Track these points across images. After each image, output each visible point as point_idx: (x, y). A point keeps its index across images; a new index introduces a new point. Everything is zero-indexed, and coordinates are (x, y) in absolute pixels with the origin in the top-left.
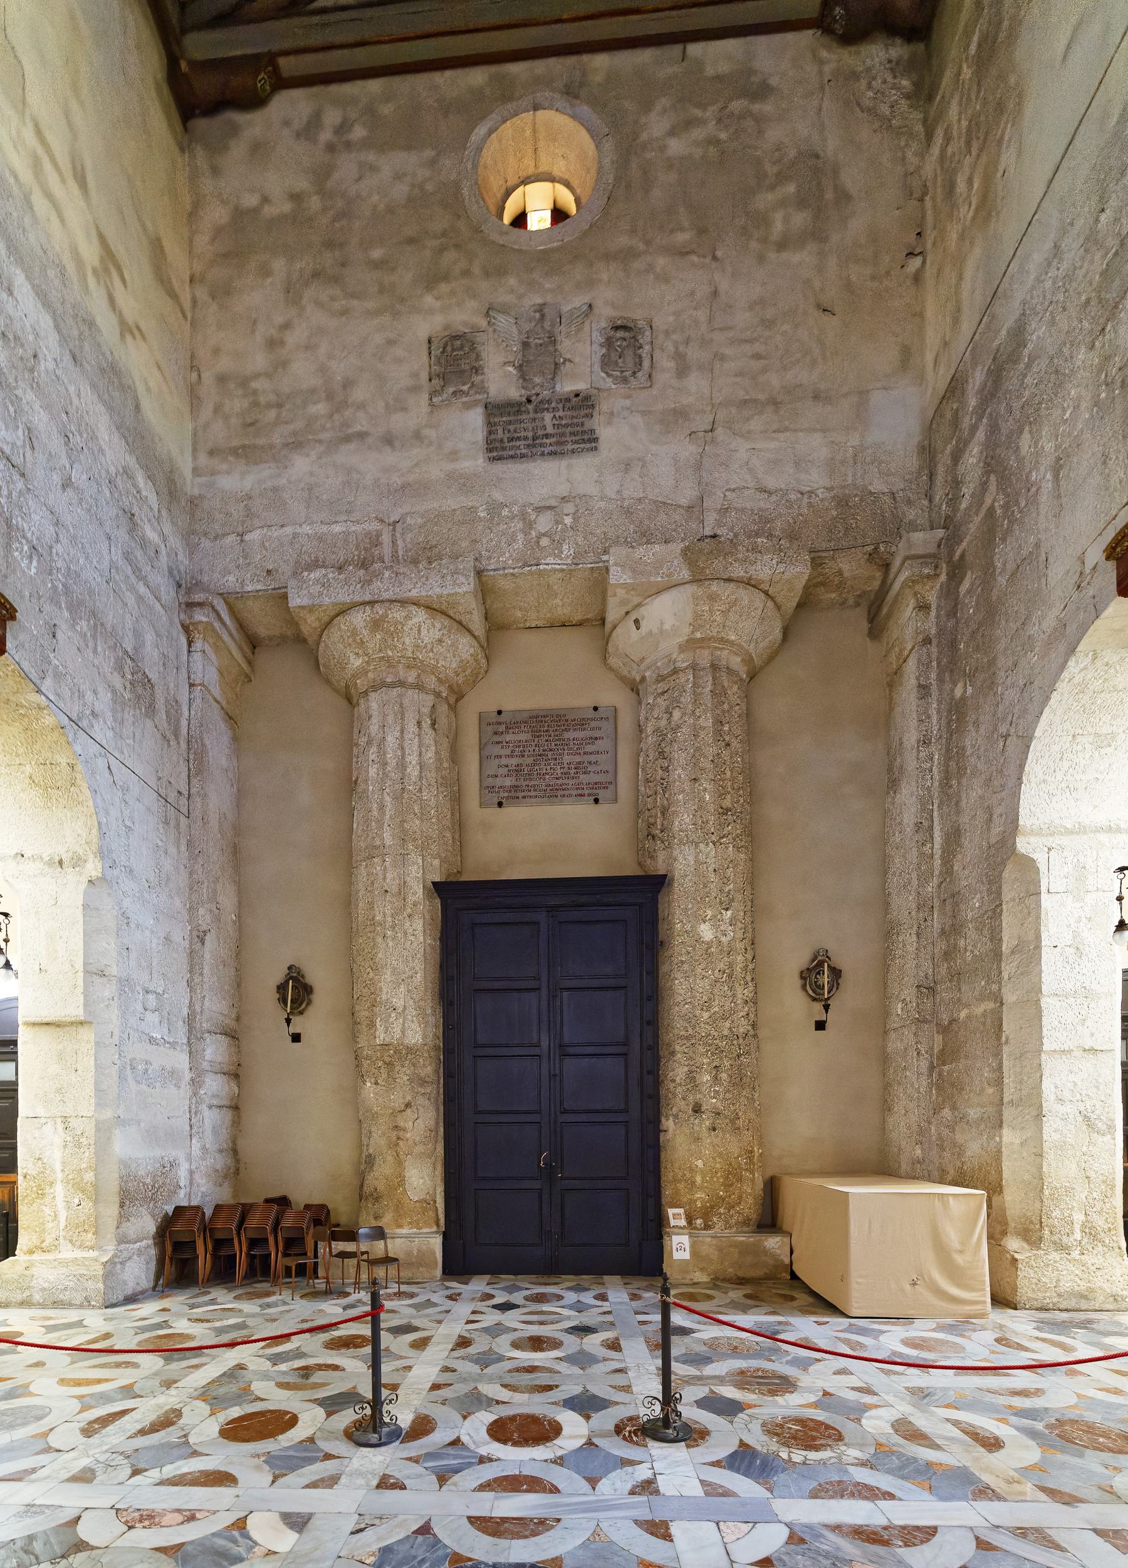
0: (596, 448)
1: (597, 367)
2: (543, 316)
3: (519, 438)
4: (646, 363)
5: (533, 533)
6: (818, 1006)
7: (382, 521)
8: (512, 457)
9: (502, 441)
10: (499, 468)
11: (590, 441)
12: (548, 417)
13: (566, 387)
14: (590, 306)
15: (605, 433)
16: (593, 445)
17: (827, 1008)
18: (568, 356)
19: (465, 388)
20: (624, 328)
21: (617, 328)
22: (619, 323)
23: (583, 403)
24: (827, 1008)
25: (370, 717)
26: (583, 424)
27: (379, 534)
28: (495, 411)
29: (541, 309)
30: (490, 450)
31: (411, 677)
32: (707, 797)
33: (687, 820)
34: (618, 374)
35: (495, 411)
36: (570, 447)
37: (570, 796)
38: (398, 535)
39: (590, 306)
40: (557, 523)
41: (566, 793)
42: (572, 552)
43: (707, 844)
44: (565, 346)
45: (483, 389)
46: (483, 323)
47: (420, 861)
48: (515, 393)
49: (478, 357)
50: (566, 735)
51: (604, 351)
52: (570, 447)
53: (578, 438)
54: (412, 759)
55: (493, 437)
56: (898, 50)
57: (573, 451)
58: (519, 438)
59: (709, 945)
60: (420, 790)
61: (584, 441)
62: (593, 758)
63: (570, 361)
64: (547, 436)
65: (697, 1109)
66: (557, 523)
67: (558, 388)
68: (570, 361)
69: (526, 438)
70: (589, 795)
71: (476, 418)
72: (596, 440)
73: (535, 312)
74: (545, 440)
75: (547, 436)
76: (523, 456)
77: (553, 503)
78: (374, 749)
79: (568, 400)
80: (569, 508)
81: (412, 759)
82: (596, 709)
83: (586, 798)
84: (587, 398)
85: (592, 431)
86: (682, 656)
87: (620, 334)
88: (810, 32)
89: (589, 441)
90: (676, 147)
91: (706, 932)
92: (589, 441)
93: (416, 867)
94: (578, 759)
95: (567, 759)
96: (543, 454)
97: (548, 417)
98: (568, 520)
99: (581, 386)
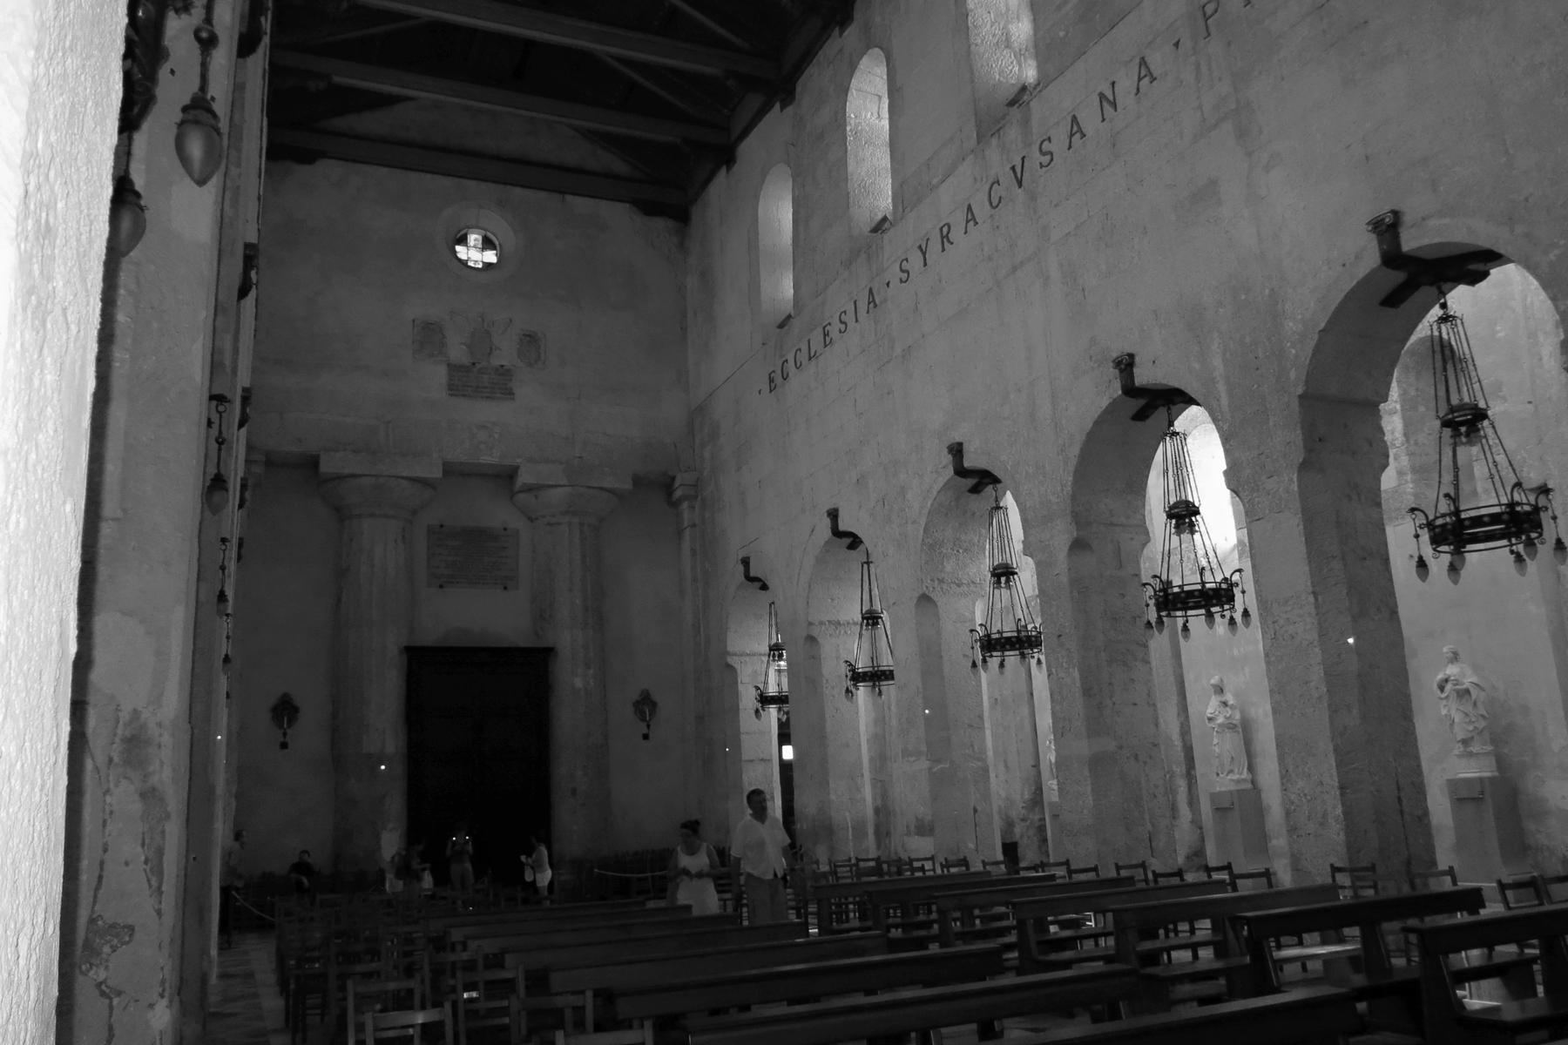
0: (513, 399)
2: (483, 320)
3: (468, 386)
6: (644, 725)
13: (496, 361)
14: (511, 320)
17: (648, 726)
20: (529, 336)
21: (525, 335)
22: (527, 333)
23: (505, 373)
24: (648, 726)
28: (453, 368)
30: (450, 389)
35: (453, 368)
39: (511, 320)
40: (490, 436)
48: (466, 361)
49: (444, 337)
58: (468, 386)
64: (486, 387)
65: (574, 792)
66: (490, 436)
69: (471, 386)
75: (486, 387)
79: (497, 369)
84: (509, 370)
85: (511, 389)
87: (528, 338)
88: (628, 205)
89: (509, 394)
92: (509, 394)
96: (482, 397)
97: (486, 377)
98: (497, 436)
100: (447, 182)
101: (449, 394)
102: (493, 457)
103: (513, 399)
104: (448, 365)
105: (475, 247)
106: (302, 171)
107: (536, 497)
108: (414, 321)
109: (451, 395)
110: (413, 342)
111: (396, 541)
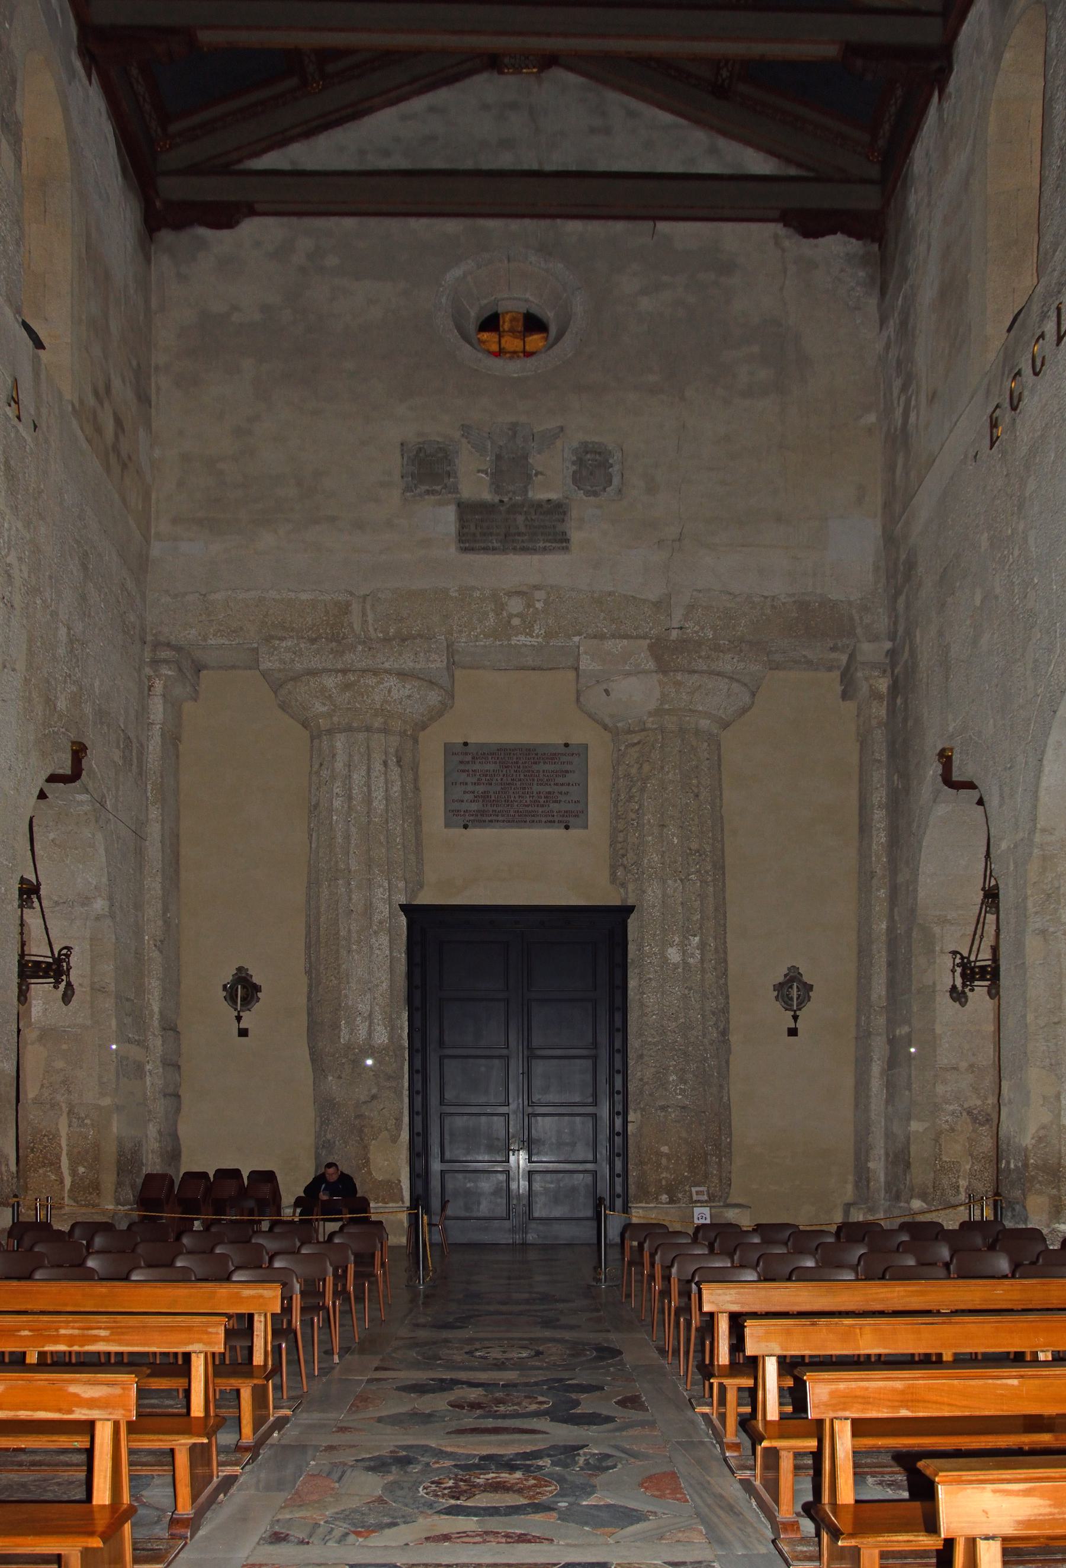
0: (567, 548)
1: (569, 481)
2: (515, 434)
4: (616, 481)
5: (505, 614)
7: (351, 594)
8: (484, 549)
9: (474, 535)
10: (470, 557)
11: (561, 541)
12: (520, 519)
15: (576, 536)
16: (564, 544)
18: (540, 469)
19: (438, 488)
25: (334, 756)
26: (554, 527)
27: (348, 604)
29: (514, 427)
30: (460, 541)
31: (378, 722)
32: (676, 841)
33: (656, 859)
34: (589, 488)
35: (467, 510)
36: (541, 544)
37: (540, 821)
38: (368, 607)
40: (529, 606)
41: (536, 819)
42: (542, 632)
43: (675, 881)
44: (537, 460)
45: (455, 490)
46: (457, 435)
47: (386, 884)
48: (487, 496)
50: (535, 767)
51: (575, 468)
52: (541, 544)
53: (550, 537)
54: (379, 795)
55: (466, 530)
56: (854, 245)
57: (545, 549)
59: (676, 966)
60: (387, 822)
61: (555, 541)
62: (564, 789)
63: (542, 473)
64: (519, 534)
67: (530, 494)
68: (542, 473)
70: (559, 822)
71: (450, 514)
72: (568, 541)
73: (509, 429)
74: (517, 537)
75: (519, 534)
76: (494, 549)
77: (525, 589)
78: (338, 783)
80: (540, 595)
81: (379, 795)
82: (566, 745)
83: (556, 824)
85: (564, 533)
86: (651, 719)
89: (562, 542)
90: (645, 304)
91: (674, 955)
92: (562, 542)
93: (381, 889)
94: (548, 789)
95: (536, 788)
96: (515, 549)
97: (520, 519)
98: (539, 605)
99: (553, 496)
100: (452, 226)
101: (461, 549)
102: (533, 637)
103: (567, 548)
104: (459, 505)
105: (512, 331)
106: (220, 241)
107: (607, 692)
108: (402, 444)
109: (465, 550)
110: (402, 477)
111: (385, 764)
